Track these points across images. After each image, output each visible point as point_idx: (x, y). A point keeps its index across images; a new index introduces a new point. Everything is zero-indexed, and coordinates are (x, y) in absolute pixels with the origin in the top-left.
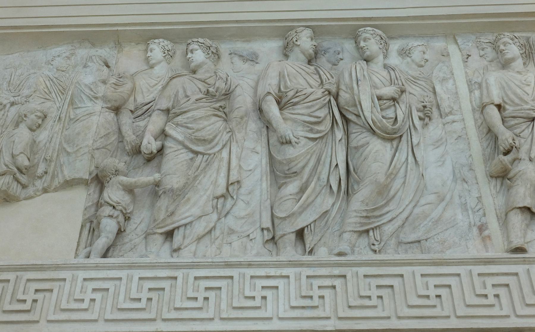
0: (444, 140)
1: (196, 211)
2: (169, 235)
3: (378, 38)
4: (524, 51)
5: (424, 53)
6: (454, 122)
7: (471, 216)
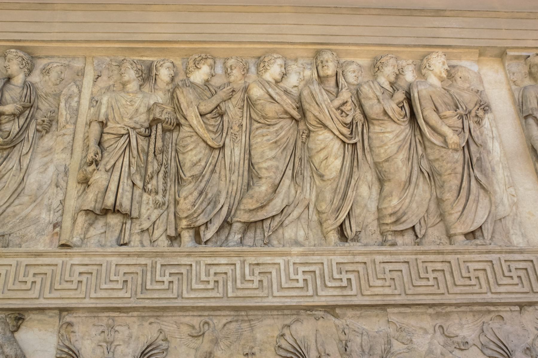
0: (53, 150)
3: (20, 59)
4: (141, 74)
6: (64, 135)
7: (51, 216)
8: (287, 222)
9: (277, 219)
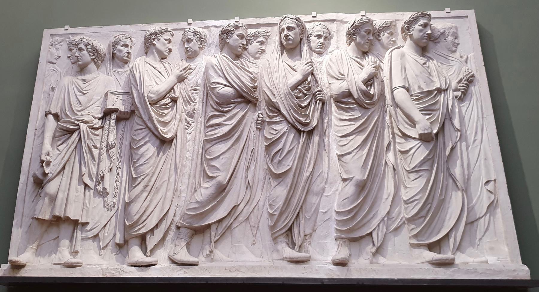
8: (234, 226)
9: (225, 224)
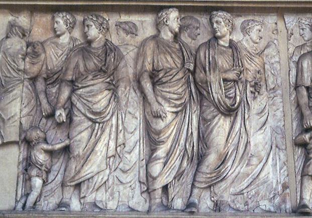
1: (94, 169)
2: (78, 186)
5: (260, 31)
